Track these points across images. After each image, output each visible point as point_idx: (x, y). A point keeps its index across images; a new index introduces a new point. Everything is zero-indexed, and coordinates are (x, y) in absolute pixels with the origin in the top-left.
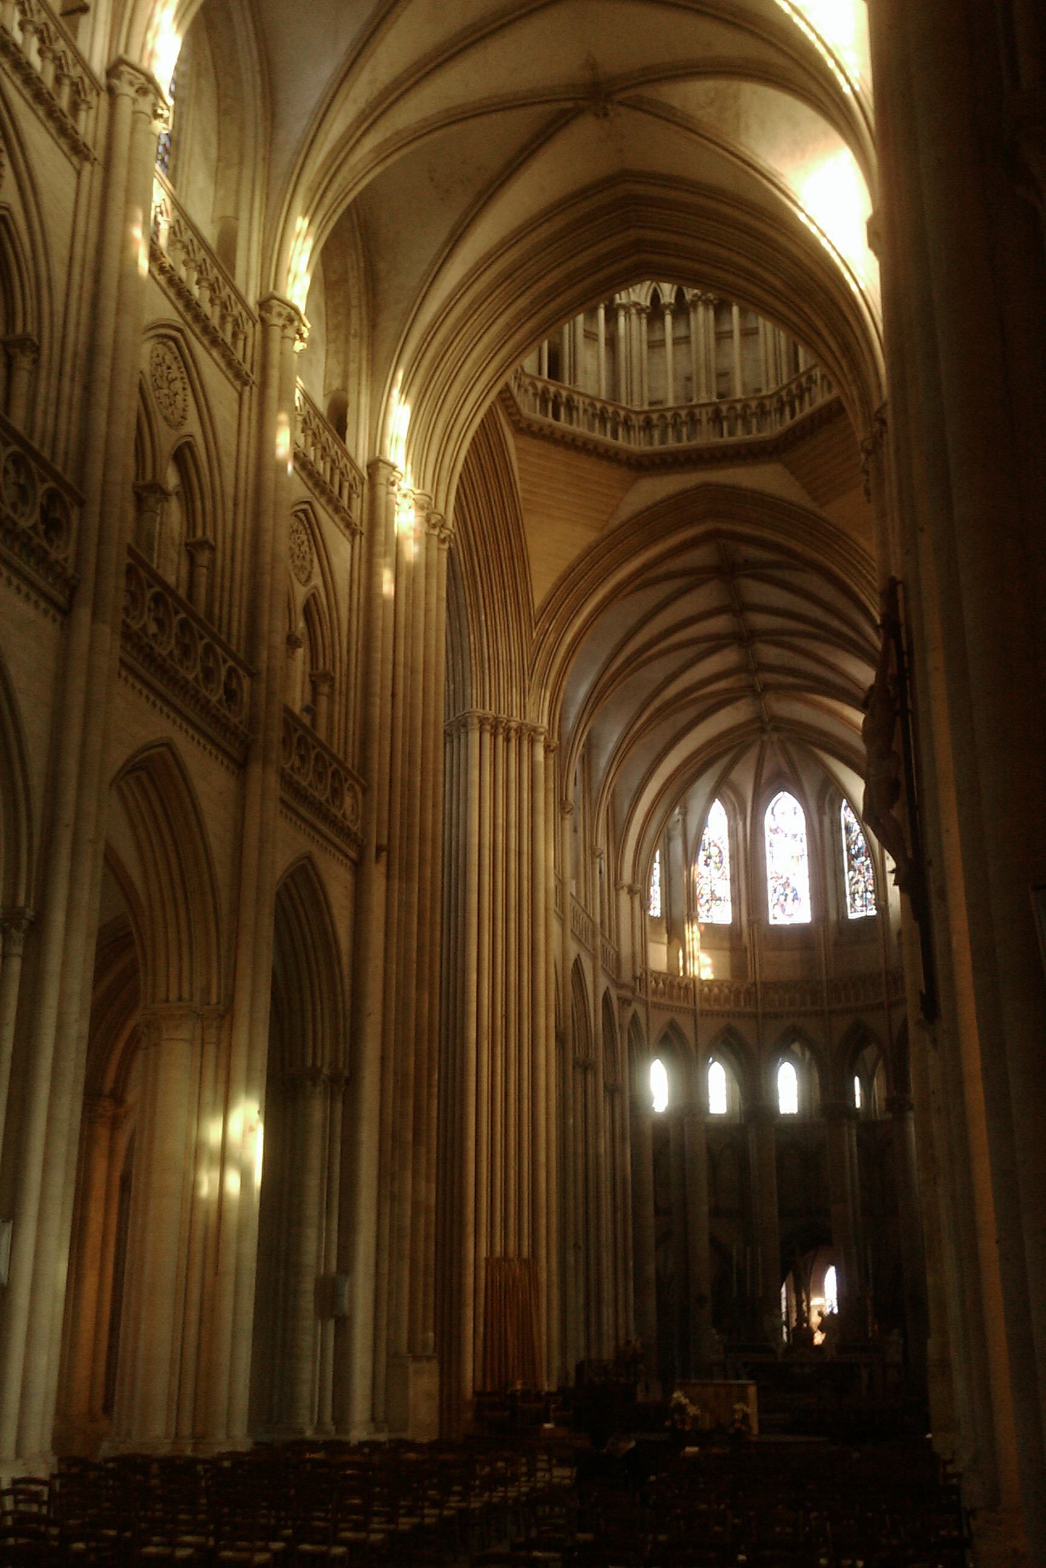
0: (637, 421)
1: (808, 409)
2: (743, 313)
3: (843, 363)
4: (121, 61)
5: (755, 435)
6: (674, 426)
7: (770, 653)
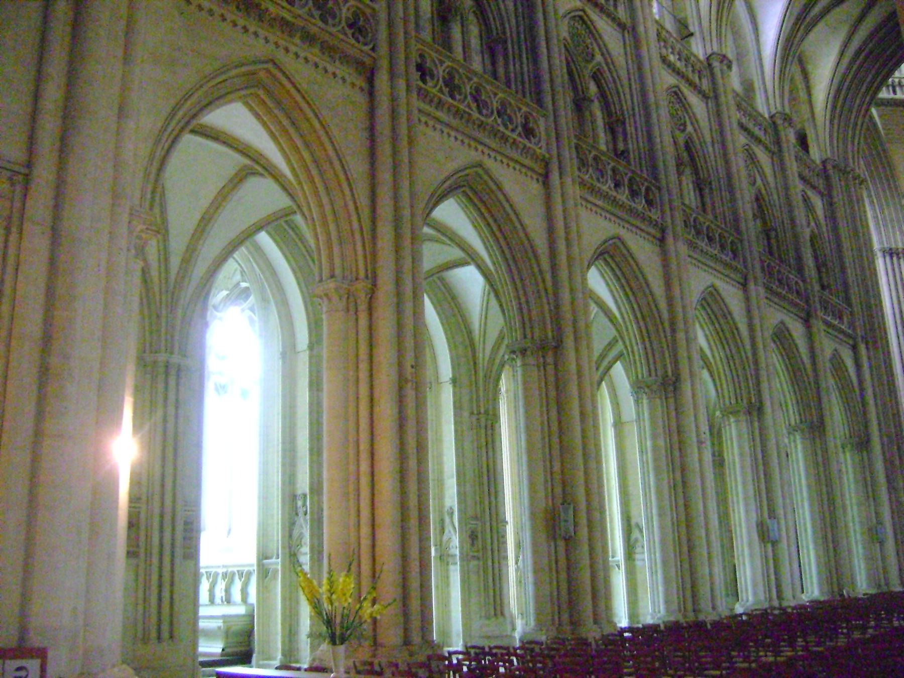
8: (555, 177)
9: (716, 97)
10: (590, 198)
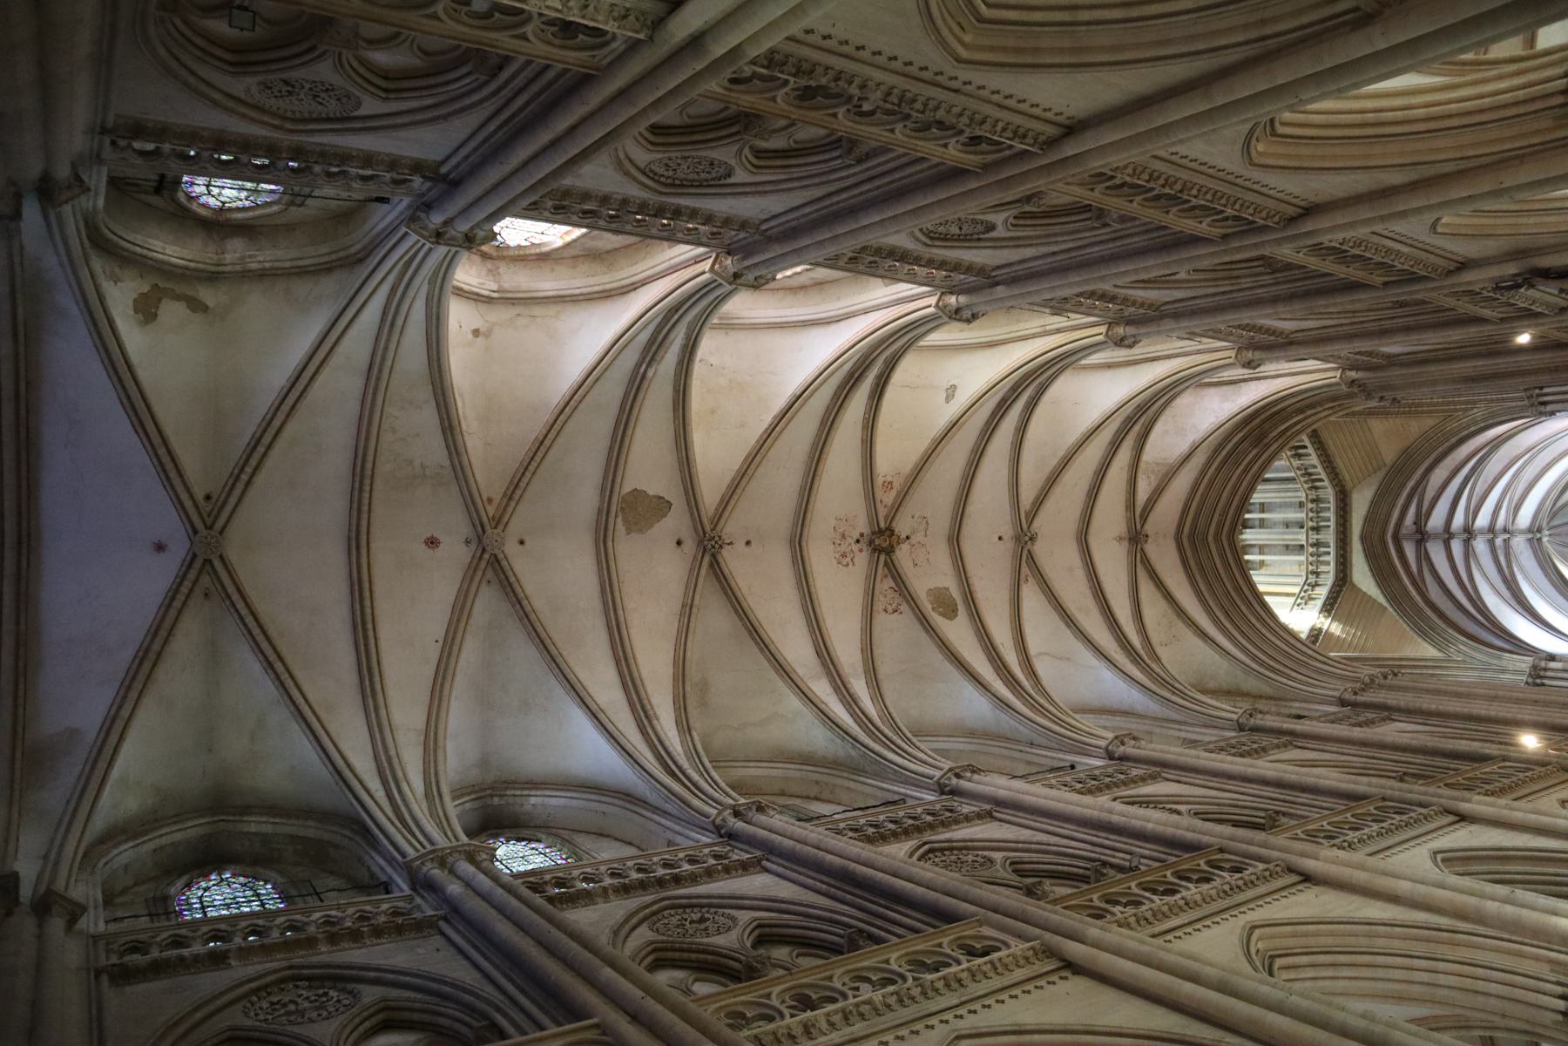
0: (1312, 579)
1: (1320, 469)
2: (1249, 512)
3: (1309, 413)
4: (1106, 749)
5: (1332, 506)
6: (1319, 556)
7: (1482, 520)
8: (1074, 949)
9: (1164, 765)
10: (1157, 930)
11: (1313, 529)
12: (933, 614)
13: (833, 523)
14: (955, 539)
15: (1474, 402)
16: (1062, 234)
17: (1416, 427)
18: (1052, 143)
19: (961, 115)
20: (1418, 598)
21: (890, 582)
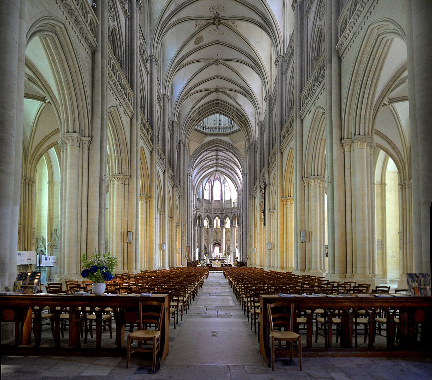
0: (207, 127)
1: (233, 130)
4: (166, 94)
7: (220, 161)
9: (164, 110)
11: (219, 128)
12: (196, 38)
13: (222, 5)
14: (217, 43)
15: (246, 163)
16: (290, 97)
17: (242, 151)
18: (301, 116)
19: (309, 102)
20: (203, 151)
21: (205, 23)
